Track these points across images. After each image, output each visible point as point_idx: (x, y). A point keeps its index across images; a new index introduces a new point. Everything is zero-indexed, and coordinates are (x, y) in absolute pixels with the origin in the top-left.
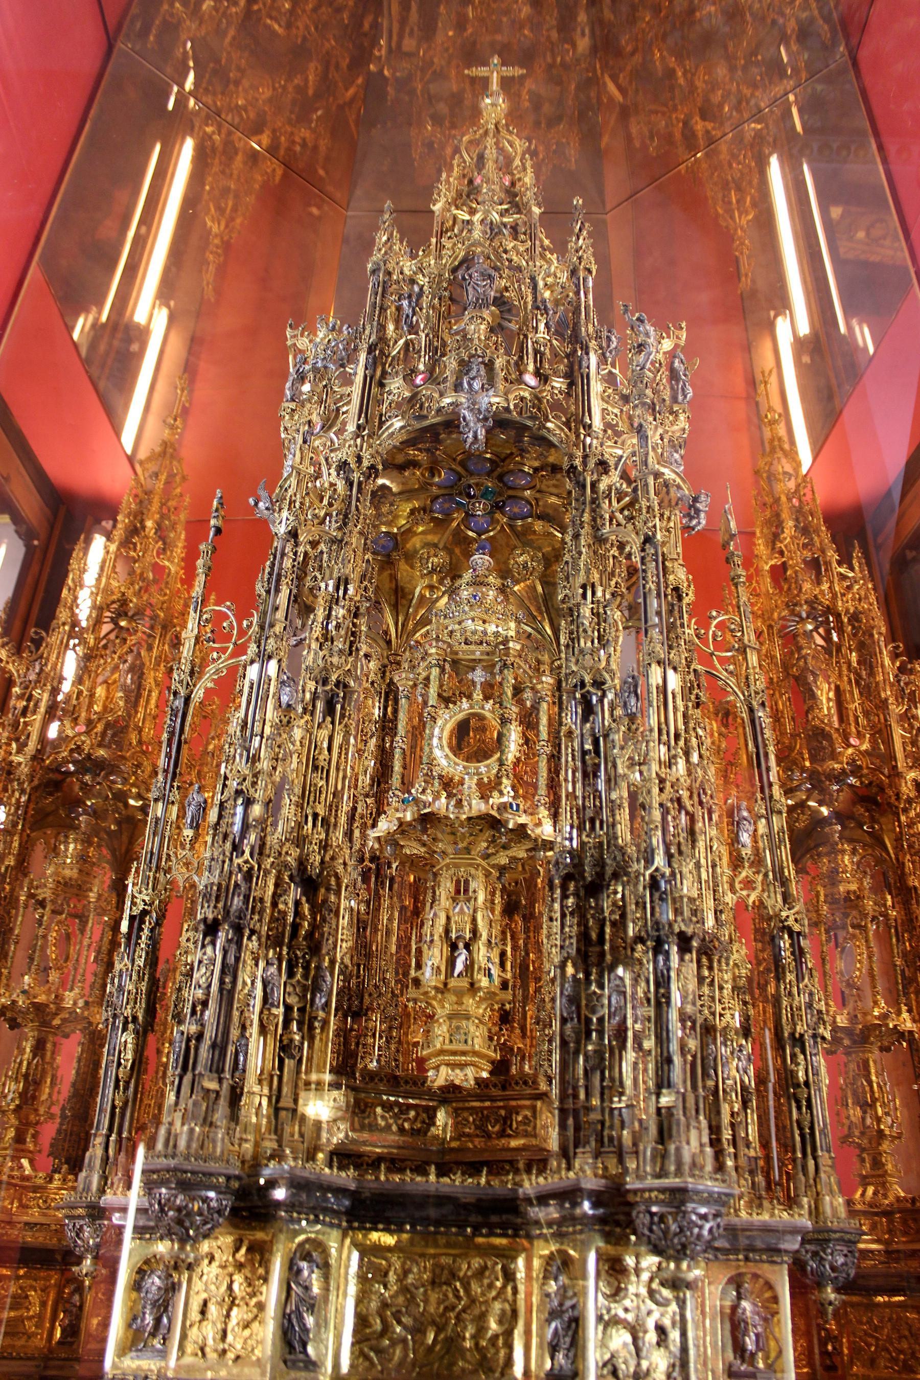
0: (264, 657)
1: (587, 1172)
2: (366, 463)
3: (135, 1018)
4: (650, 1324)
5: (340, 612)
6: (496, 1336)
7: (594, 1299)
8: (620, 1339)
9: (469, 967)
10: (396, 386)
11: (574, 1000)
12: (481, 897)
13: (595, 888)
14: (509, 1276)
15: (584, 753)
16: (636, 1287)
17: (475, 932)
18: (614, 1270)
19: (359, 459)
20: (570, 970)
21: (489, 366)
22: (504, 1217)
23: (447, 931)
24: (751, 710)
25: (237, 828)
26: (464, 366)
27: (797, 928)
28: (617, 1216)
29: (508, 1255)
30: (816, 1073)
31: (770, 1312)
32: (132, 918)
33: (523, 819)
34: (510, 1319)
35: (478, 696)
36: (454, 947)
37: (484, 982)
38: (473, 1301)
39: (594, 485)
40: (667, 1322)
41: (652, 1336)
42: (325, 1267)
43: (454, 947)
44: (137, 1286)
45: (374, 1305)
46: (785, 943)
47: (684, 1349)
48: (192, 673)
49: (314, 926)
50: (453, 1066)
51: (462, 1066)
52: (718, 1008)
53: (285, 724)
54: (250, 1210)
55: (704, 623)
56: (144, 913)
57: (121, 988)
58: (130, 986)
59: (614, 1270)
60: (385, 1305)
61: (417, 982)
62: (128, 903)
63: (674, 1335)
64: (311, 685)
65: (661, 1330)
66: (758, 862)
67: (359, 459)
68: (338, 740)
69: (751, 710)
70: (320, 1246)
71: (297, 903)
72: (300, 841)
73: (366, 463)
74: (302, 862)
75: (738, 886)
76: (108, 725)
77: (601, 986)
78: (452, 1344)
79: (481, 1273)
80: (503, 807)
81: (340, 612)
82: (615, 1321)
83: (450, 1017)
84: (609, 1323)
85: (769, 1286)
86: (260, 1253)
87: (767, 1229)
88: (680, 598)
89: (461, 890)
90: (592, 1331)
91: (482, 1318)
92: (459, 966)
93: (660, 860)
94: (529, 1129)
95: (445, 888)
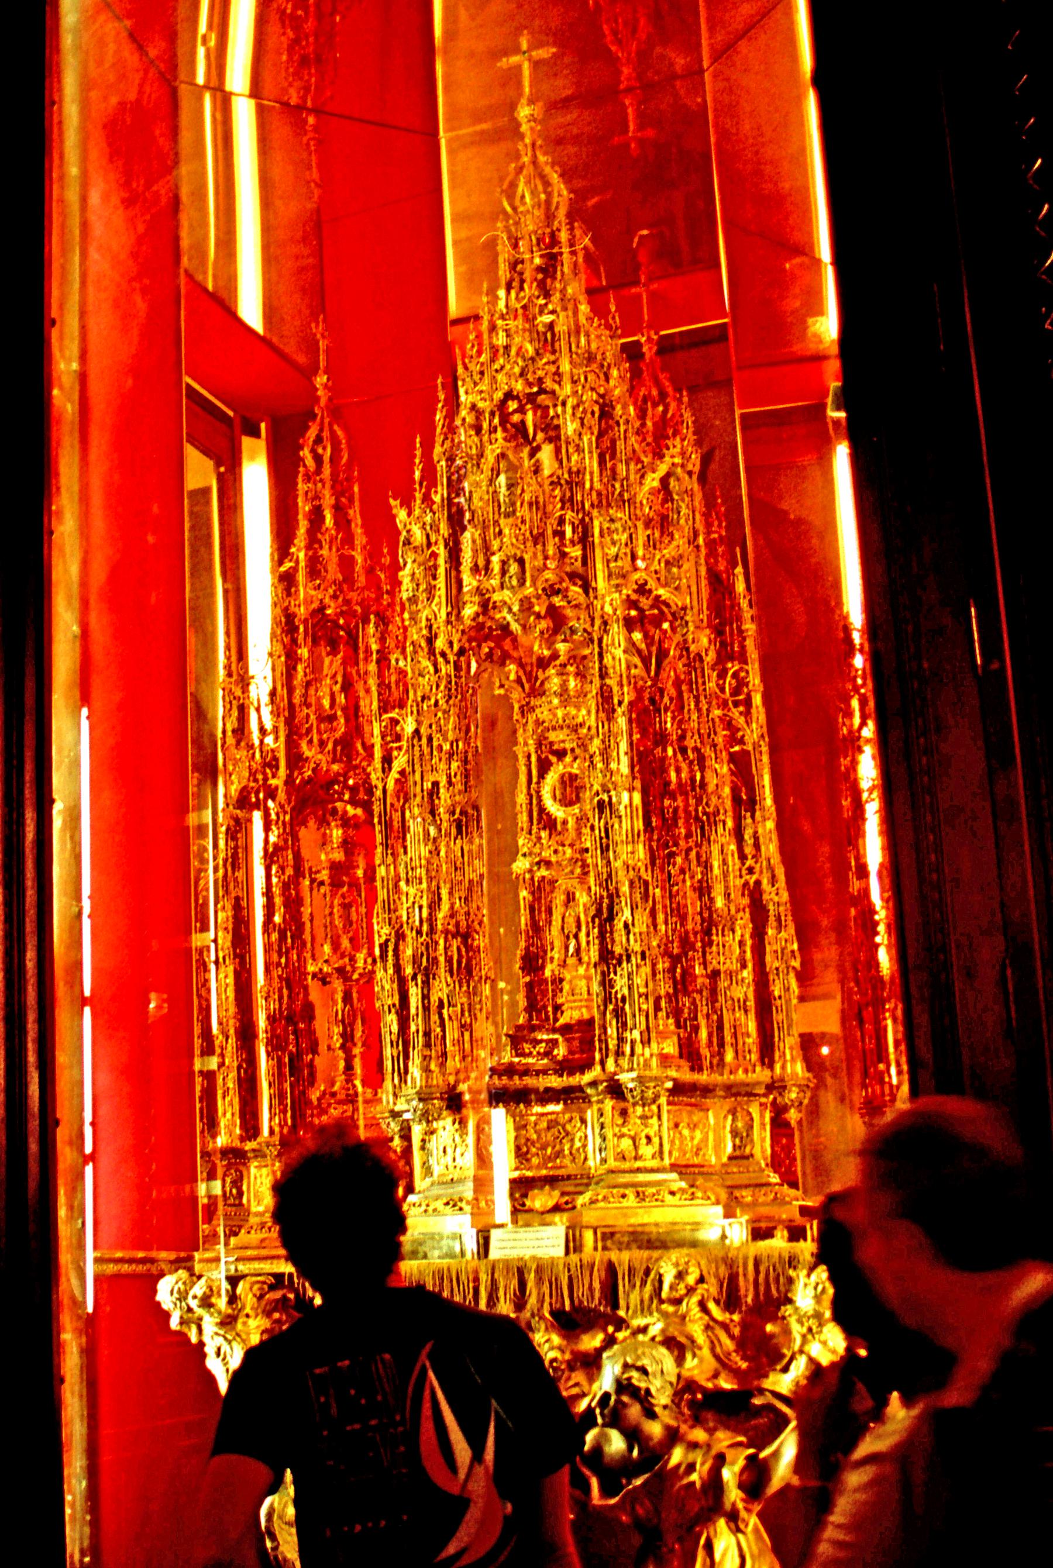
2: (456, 647)
3: (394, 1005)
4: (643, 1135)
6: (578, 1150)
8: (626, 1144)
11: (603, 983)
15: (601, 838)
19: (451, 644)
25: (417, 923)
27: (776, 899)
32: (381, 945)
36: (568, 937)
38: (567, 1134)
40: (652, 1134)
41: (644, 1141)
45: (523, 1141)
47: (661, 1145)
48: (383, 771)
49: (469, 960)
52: (722, 959)
54: (454, 1103)
55: (722, 675)
56: (387, 941)
57: (383, 988)
58: (387, 987)
62: (376, 936)
63: (656, 1140)
65: (649, 1138)
67: (451, 644)
71: (458, 948)
72: (453, 915)
73: (456, 647)
75: (744, 872)
76: (336, 743)
77: (615, 974)
79: (571, 1120)
81: (454, 765)
82: (623, 1136)
85: (750, 1114)
88: (702, 660)
91: (572, 1140)
92: (571, 950)
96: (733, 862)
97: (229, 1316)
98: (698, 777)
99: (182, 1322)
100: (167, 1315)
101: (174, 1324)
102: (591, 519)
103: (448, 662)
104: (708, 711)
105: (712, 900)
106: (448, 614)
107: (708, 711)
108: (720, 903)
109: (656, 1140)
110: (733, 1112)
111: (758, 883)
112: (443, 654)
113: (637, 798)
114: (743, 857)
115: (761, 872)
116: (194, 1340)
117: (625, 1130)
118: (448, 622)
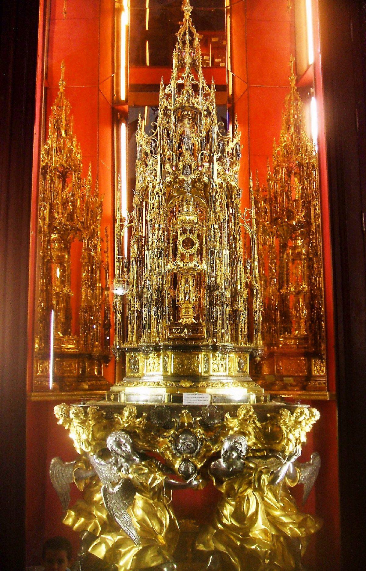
0: (148, 250)
1: (210, 342)
5: (160, 232)
7: (211, 361)
8: (216, 366)
9: (189, 298)
10: (168, 166)
11: (209, 312)
12: (191, 283)
13: (214, 290)
14: (198, 358)
16: (219, 358)
17: (190, 290)
18: (214, 356)
19: (161, 190)
20: (208, 307)
21: (190, 166)
22: (198, 349)
23: (184, 290)
24: (252, 235)
26: (184, 167)
28: (215, 348)
29: (198, 355)
30: (259, 318)
31: (246, 362)
33: (200, 267)
34: (198, 364)
35: (188, 233)
37: (192, 302)
39: (215, 196)
42: (168, 357)
43: (185, 294)
44: (129, 361)
46: (255, 291)
50: (186, 318)
51: (188, 318)
53: (153, 261)
54: (157, 349)
58: (118, 305)
59: (214, 356)
60: (178, 363)
61: (178, 301)
63: (224, 366)
64: (156, 250)
65: (222, 365)
66: (251, 273)
67: (161, 190)
68: (163, 262)
69: (252, 235)
70: (168, 354)
74: (159, 287)
78: (190, 368)
80: (195, 266)
83: (186, 308)
84: (214, 364)
85: (246, 357)
86: (159, 356)
87: (245, 348)
89: (187, 282)
90: (211, 365)
93: (223, 290)
94: (202, 332)
95: (184, 280)
96: (243, 275)
97: (84, 420)
98: (234, 245)
99: (65, 422)
100: (58, 420)
101: (60, 422)
102: (213, 155)
103: (159, 196)
104: (238, 223)
105: (236, 286)
106: (160, 180)
107: (238, 223)
108: (239, 287)
109: (224, 366)
110: (240, 357)
111: (250, 282)
112: (157, 193)
113: (228, 252)
114: (246, 272)
115: (252, 278)
116: (66, 428)
117: (215, 362)
118: (160, 182)
